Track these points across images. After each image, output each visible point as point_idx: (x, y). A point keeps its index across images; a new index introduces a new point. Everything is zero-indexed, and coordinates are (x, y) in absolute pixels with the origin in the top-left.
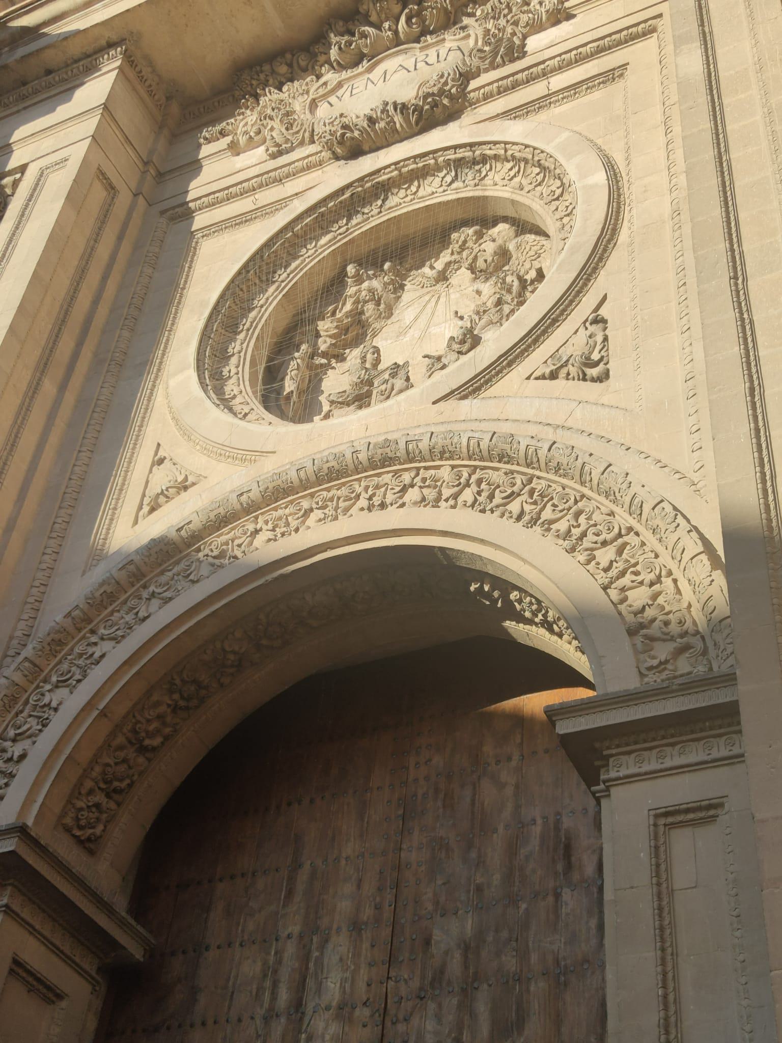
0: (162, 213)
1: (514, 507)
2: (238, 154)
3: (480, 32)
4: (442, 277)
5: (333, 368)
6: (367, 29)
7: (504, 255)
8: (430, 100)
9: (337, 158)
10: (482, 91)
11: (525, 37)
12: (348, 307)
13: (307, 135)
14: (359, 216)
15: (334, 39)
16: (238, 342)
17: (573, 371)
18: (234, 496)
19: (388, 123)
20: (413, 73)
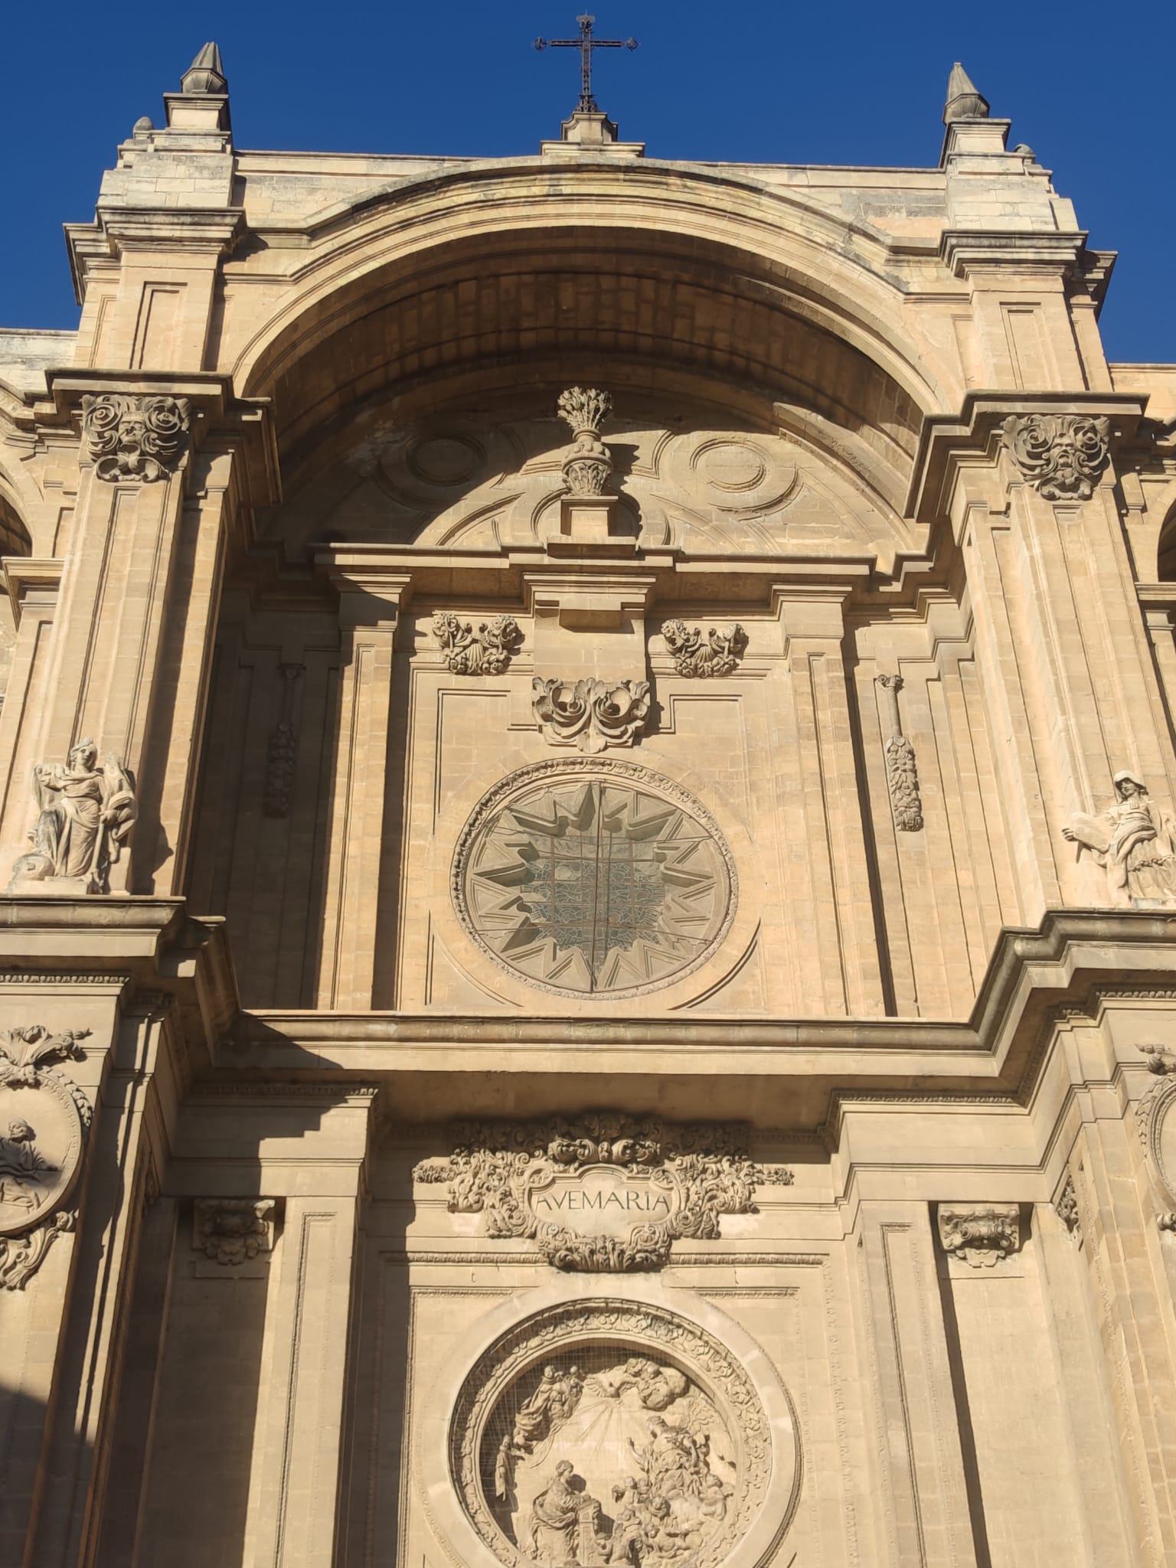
0: (381, 1252)
2: (453, 1212)
3: (683, 1191)
4: (617, 1395)
6: (587, 1142)
7: (671, 1398)
9: (551, 1264)
12: (539, 1402)
13: (528, 1232)
15: (558, 1141)
16: (466, 1444)
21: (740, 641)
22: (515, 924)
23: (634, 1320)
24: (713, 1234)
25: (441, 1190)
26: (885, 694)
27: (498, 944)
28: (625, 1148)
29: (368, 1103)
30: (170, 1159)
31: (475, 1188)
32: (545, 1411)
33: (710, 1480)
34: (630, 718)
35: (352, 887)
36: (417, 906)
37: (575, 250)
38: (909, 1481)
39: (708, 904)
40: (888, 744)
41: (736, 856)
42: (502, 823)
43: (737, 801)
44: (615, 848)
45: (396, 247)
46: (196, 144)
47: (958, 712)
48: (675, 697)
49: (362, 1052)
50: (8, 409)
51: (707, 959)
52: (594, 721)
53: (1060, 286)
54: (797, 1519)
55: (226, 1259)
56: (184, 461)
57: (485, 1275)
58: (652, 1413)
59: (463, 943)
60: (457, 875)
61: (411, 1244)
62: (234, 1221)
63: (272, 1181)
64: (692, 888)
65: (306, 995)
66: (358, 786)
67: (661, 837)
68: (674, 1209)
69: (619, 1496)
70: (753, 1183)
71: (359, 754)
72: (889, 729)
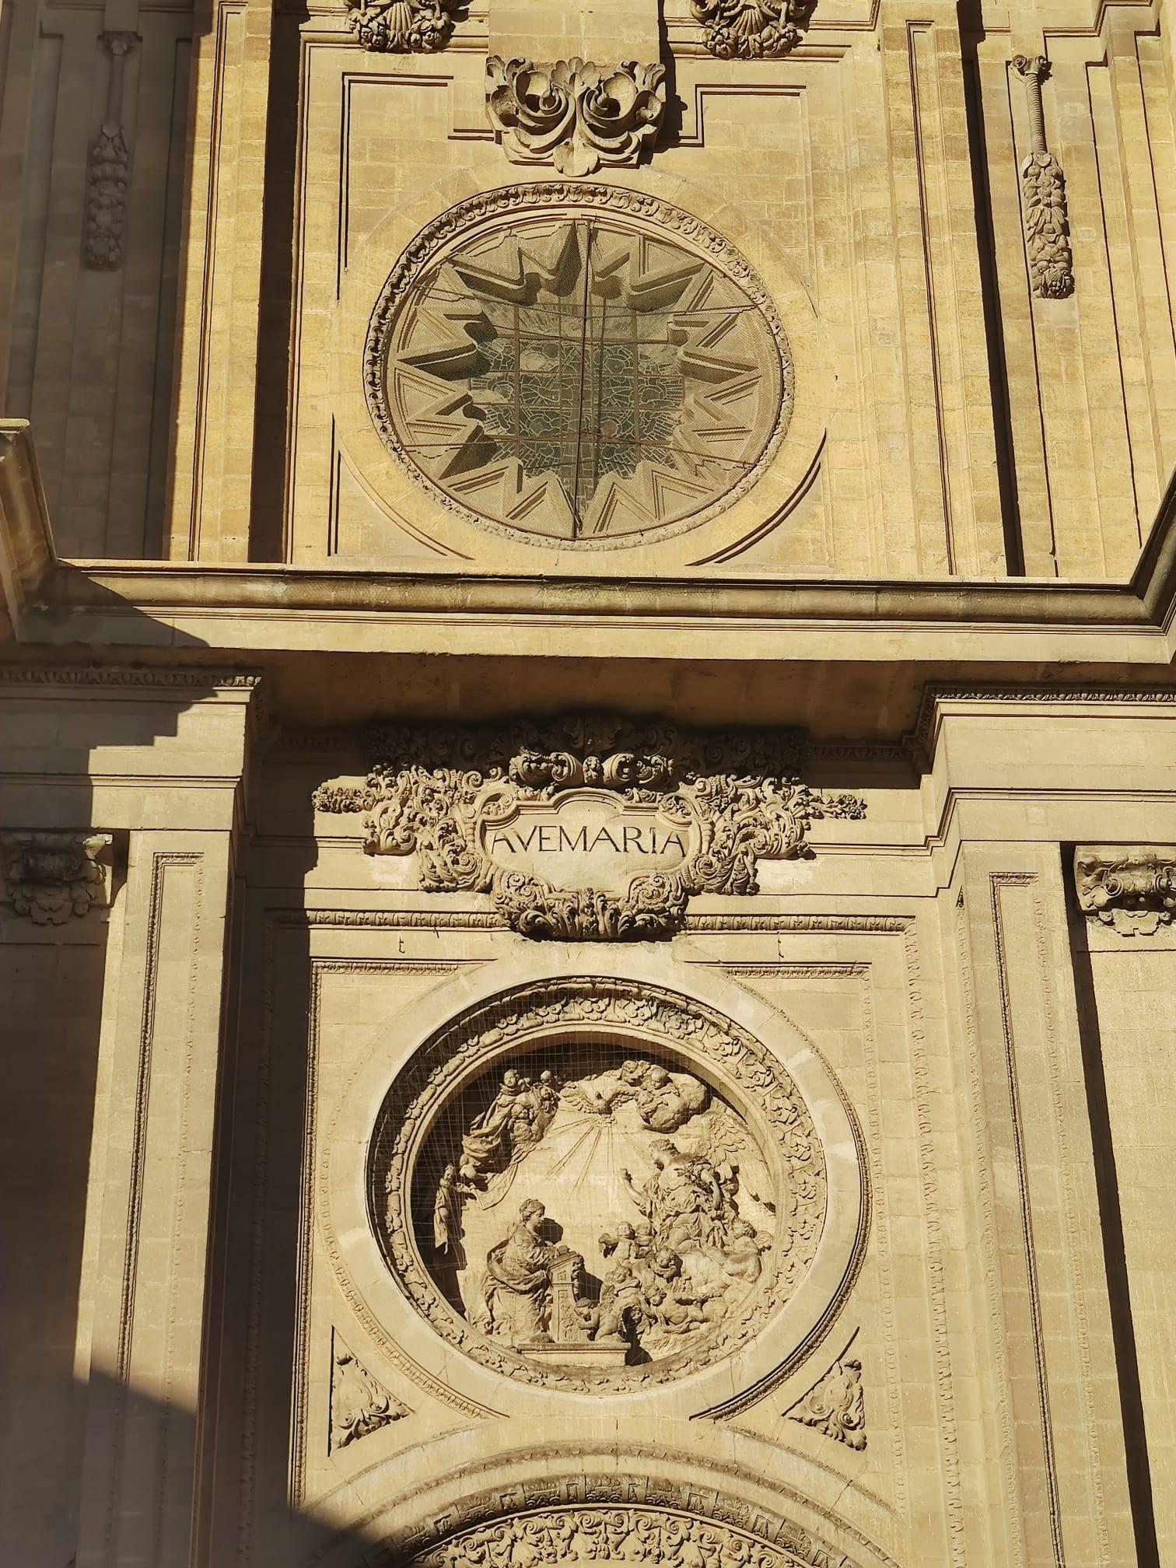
2: (372, 855)
4: (608, 1110)
5: (473, 1197)
6: (565, 756)
8: (647, 917)
9: (514, 928)
10: (703, 919)
11: (756, 859)
12: (496, 1120)
13: (480, 883)
14: (530, 1015)
15: (525, 754)
16: (394, 1171)
17: (833, 1430)
18: (496, 1496)
19: (591, 923)
20: (623, 854)
22: (461, 437)
23: (632, 1007)
24: (748, 887)
25: (353, 824)
26: (1022, 86)
27: (436, 467)
28: (622, 765)
29: (246, 697)
31: (403, 821)
32: (505, 1133)
33: (739, 1228)
34: (635, 121)
35: (218, 377)
36: (314, 408)
38: (1021, 1231)
39: (748, 409)
40: (1024, 165)
41: (792, 335)
42: (441, 283)
43: (795, 251)
44: (611, 323)
47: (1132, 115)
48: (704, 89)
49: (235, 623)
51: (746, 491)
52: (581, 125)
54: (861, 1282)
55: (42, 917)
57: (419, 943)
58: (658, 1136)
60: (373, 363)
61: (311, 900)
63: (109, 808)
64: (725, 385)
65: (155, 541)
66: (224, 224)
67: (678, 307)
68: (692, 852)
69: (609, 1249)
70: (806, 816)
71: (224, 174)
72: (1027, 140)
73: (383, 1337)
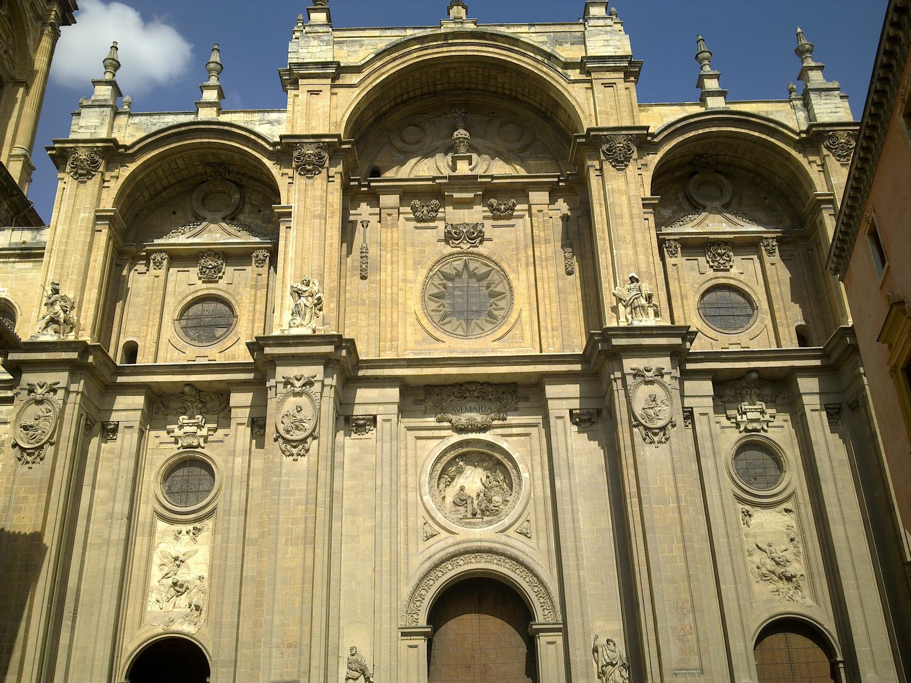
1: (518, 571)
21: (514, 205)
22: (441, 313)
30: (341, 404)
37: (454, 62)
45: (392, 68)
46: (321, 29)
48: (494, 226)
50: (268, 146)
53: (622, 75)
56: (327, 164)
57: (437, 433)
59: (425, 322)
62: (362, 422)
66: (389, 268)
73: (433, 518)
